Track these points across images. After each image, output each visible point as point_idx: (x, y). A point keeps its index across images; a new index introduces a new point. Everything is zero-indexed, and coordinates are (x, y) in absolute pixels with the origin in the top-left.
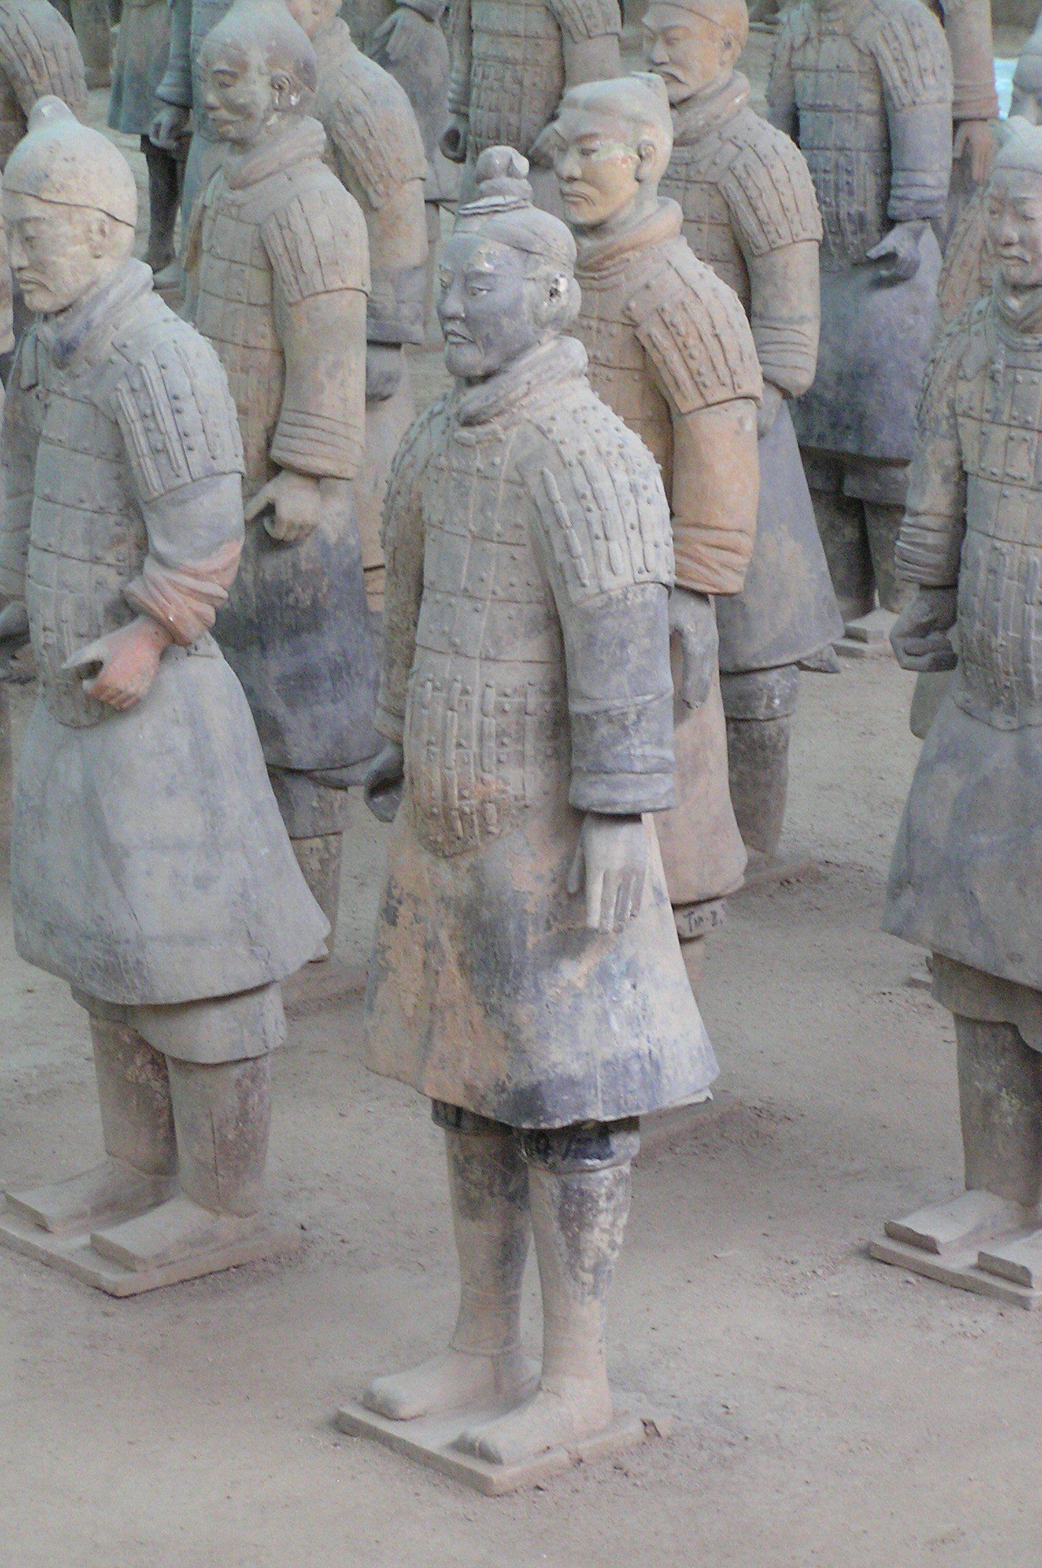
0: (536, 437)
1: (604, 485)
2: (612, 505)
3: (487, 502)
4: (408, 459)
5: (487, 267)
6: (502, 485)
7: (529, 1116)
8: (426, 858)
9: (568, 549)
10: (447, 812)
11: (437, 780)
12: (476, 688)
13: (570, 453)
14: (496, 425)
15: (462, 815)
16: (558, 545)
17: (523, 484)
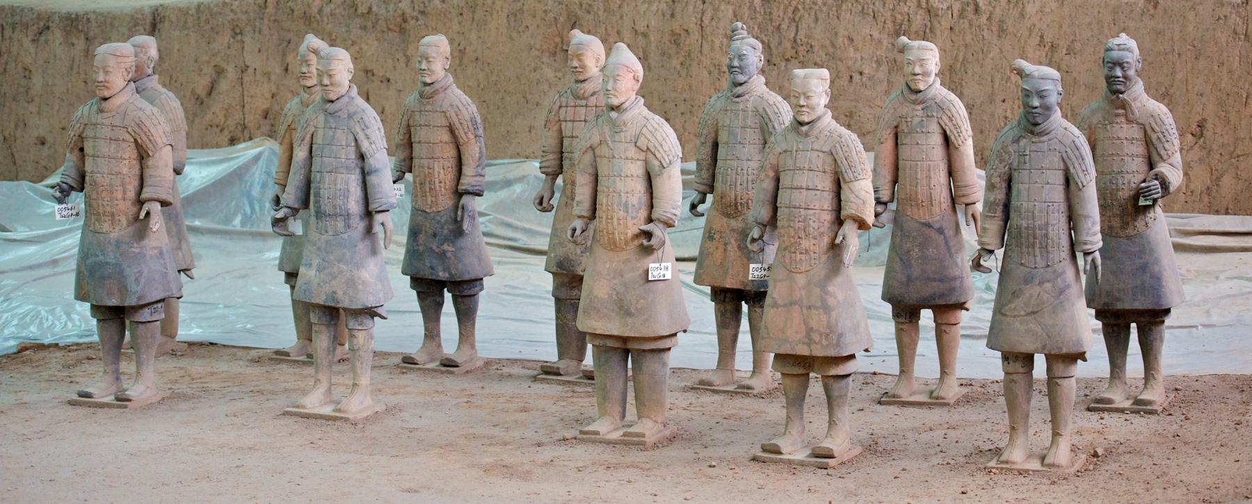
0: (760, 99)
1: (781, 110)
2: (784, 114)
3: (745, 118)
4: (712, 110)
5: (745, 52)
6: (750, 113)
7: (763, 287)
8: (725, 220)
9: (774, 128)
10: (736, 204)
11: (733, 197)
12: (745, 168)
13: (771, 103)
14: (747, 97)
15: (741, 203)
16: (770, 126)
17: (757, 111)
